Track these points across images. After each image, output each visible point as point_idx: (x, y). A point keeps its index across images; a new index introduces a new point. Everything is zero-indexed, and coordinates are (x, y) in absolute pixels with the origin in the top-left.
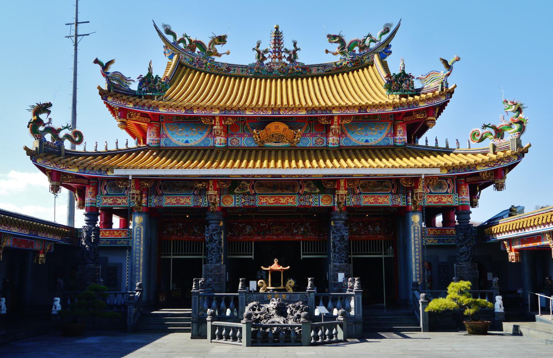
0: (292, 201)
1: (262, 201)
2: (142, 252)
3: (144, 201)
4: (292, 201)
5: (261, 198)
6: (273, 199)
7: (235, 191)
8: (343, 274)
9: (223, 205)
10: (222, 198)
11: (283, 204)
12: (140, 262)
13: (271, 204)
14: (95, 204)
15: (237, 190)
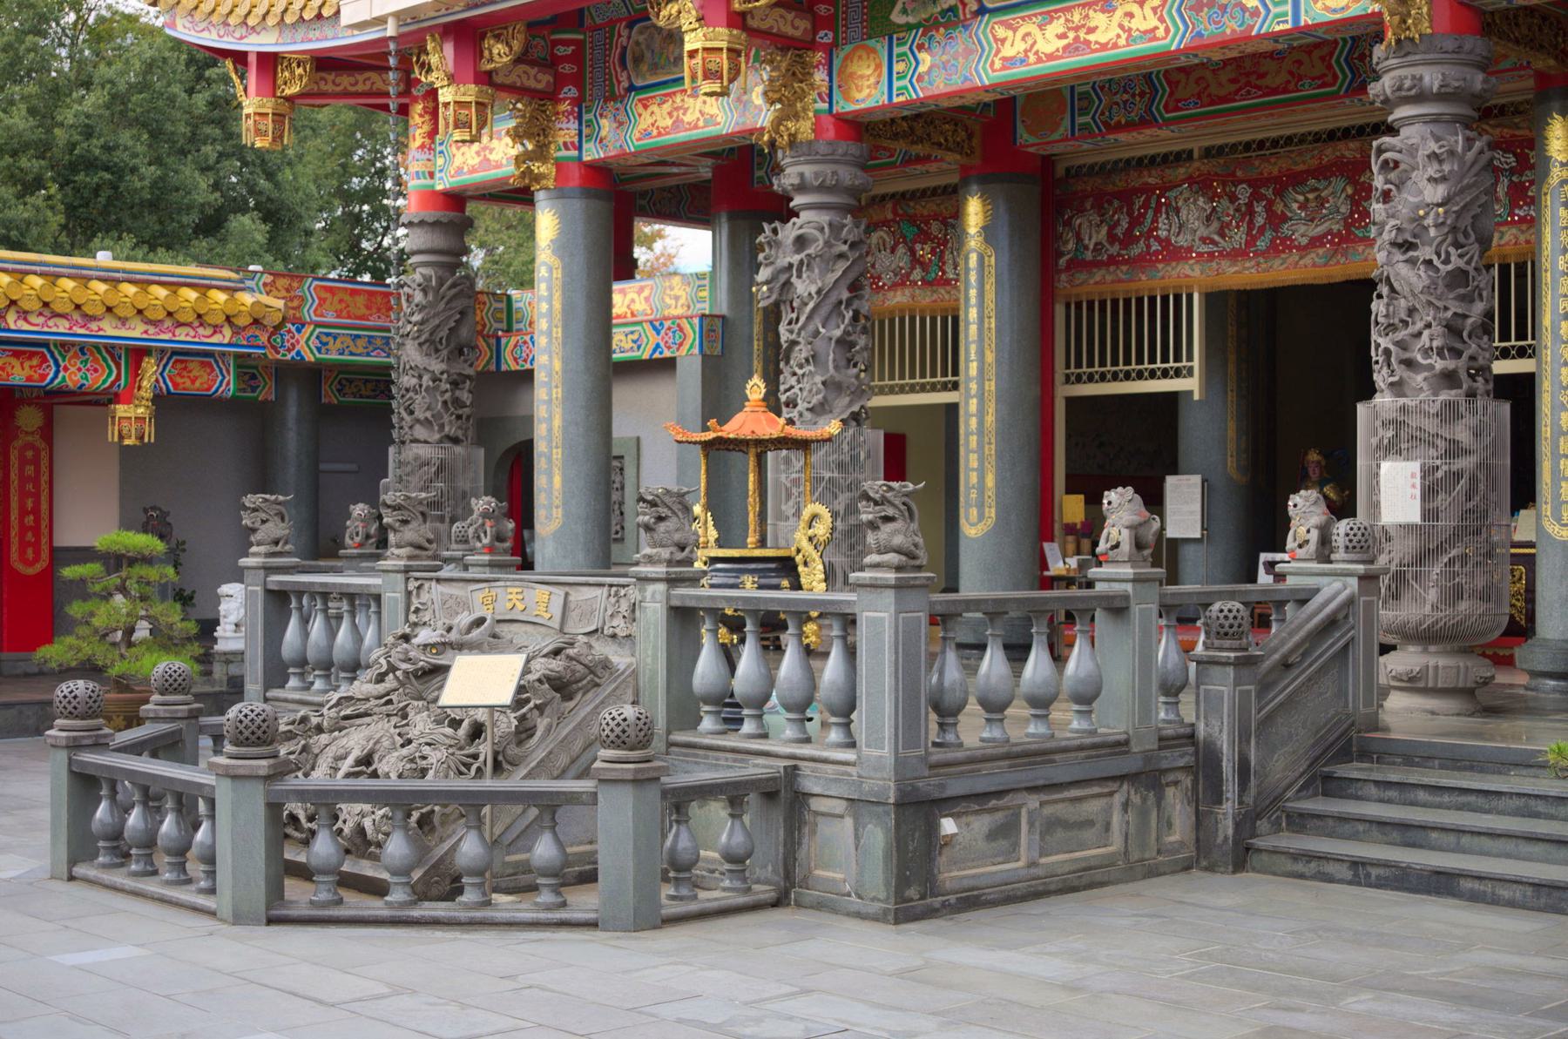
0: (1153, 22)
1: (1008, 51)
2: (557, 379)
3: (567, 130)
4: (1153, 22)
5: (1001, 32)
6: (1057, 26)
7: (897, 17)
8: (1415, 467)
9: (843, 106)
10: (837, 63)
11: (1104, 47)
12: (550, 430)
13: (1051, 57)
14: (431, 175)
15: (904, 11)
